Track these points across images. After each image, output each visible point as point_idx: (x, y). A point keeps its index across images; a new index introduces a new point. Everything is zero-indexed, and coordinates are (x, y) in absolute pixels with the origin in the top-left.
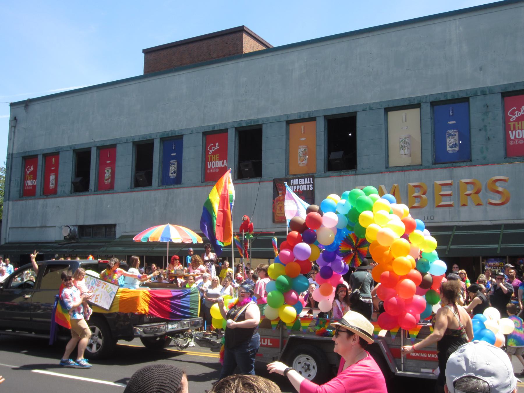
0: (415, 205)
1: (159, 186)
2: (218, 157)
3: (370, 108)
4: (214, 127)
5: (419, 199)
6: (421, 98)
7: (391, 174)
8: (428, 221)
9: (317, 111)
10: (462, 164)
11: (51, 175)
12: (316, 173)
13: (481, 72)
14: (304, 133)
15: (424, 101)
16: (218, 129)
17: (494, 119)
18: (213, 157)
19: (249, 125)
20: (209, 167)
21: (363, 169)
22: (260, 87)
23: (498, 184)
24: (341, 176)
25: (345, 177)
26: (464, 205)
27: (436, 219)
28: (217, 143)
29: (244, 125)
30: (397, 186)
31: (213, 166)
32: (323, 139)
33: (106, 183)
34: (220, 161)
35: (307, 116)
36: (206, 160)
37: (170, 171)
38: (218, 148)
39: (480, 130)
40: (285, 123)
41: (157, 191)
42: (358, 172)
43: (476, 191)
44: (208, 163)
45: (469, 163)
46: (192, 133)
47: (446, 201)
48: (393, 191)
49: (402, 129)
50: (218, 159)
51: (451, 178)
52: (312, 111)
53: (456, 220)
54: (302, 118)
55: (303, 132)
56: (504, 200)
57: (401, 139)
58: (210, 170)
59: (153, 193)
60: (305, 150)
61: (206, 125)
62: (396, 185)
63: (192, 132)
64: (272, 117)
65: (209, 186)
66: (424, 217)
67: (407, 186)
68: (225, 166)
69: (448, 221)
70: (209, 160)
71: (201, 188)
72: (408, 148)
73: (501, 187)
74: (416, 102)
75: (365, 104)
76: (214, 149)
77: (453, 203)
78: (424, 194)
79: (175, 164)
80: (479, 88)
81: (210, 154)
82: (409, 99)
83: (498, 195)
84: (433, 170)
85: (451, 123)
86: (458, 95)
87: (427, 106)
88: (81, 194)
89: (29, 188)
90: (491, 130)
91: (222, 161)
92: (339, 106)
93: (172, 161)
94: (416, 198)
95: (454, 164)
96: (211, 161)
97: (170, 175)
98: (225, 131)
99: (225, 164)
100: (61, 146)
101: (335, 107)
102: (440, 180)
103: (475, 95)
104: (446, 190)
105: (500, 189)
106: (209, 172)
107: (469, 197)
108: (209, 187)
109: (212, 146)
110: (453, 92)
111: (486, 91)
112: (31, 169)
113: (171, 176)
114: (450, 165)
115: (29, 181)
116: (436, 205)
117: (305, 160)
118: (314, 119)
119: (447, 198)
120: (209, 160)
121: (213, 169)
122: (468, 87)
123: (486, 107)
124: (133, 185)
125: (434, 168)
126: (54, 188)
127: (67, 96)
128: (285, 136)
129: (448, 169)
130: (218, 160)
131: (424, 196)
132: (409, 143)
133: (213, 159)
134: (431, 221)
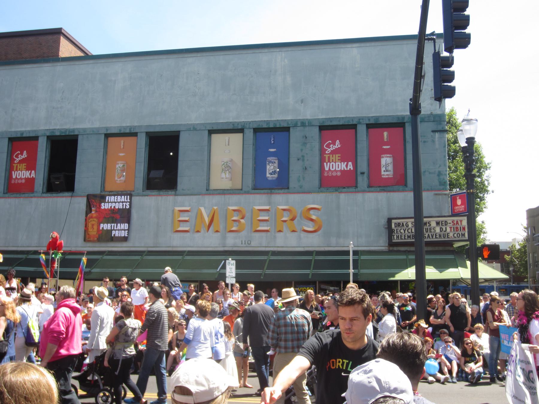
0: (234, 229)
1: (43, 193)
2: (340, 158)
3: (194, 128)
4: (377, 118)
5: (237, 223)
6: (245, 123)
7: (211, 196)
8: (245, 245)
9: (360, 119)
10: (280, 191)
11: (383, 157)
12: (242, 189)
13: (302, 104)
14: (123, 148)
15: (248, 126)
16: (28, 135)
17: (312, 150)
18: (333, 157)
19: (64, 134)
20: (327, 169)
21: (183, 190)
22: (78, 95)
23: (312, 212)
24: (160, 195)
25: (164, 197)
26: (280, 231)
27: (253, 244)
28: (338, 141)
29: (58, 134)
30: (217, 209)
31: (333, 168)
32: (144, 156)
33: (118, 182)
34: (342, 163)
35: (231, 127)
36: (322, 160)
37: (267, 171)
38: (339, 146)
39: (298, 160)
40: (103, 136)
41: (192, 197)
42: (359, 189)
43: (291, 217)
44: (325, 164)
45: (286, 191)
46: (195, 129)
47: (264, 226)
48: (212, 215)
49: (225, 152)
50: (339, 160)
51: (269, 204)
52: (134, 126)
53: (272, 246)
54: (122, 132)
55: (122, 147)
56: (316, 228)
57: (223, 163)
58: (328, 172)
59: (359, 196)
60: (123, 166)
61: (13, 130)
62: (215, 208)
63: (304, 124)
64: (90, 128)
65: (217, 194)
66: (242, 241)
67: (226, 210)
68: (350, 169)
69: (264, 245)
70: (327, 161)
71: (251, 197)
72: (230, 172)
73: (313, 215)
74: (240, 127)
75: (190, 124)
76: (333, 148)
77: (270, 229)
78: (243, 218)
79: (275, 163)
80: (300, 119)
81: (326, 152)
82: (233, 123)
83: (311, 222)
84: (253, 195)
85: (388, 147)
86: (280, 125)
87: (250, 132)
88: (61, 194)
89: (20, 181)
90: (308, 160)
91: (346, 163)
92: (162, 124)
93: (270, 159)
94: (235, 222)
95: (273, 191)
96: (329, 161)
97: (268, 175)
98: (354, 127)
99: (350, 166)
100: (351, 116)
101: (158, 124)
102: (259, 205)
103: (296, 126)
104: (264, 216)
105: (314, 217)
106: (326, 174)
107: (285, 223)
108: (12, 199)
109: (330, 144)
110: (275, 120)
111: (306, 123)
112: (22, 154)
113: (268, 177)
114: (269, 191)
115: (20, 172)
116: (254, 230)
117: (123, 176)
118: (241, 131)
119: (265, 223)
120: (327, 161)
121: (332, 172)
122: (289, 118)
123: (305, 137)
124: (45, 190)
125: (254, 194)
126: (392, 176)
127: (266, 50)
128: (102, 150)
129: (266, 195)
130: (340, 161)
131: (242, 221)
132: (231, 166)
133: (333, 160)
134: (248, 245)
